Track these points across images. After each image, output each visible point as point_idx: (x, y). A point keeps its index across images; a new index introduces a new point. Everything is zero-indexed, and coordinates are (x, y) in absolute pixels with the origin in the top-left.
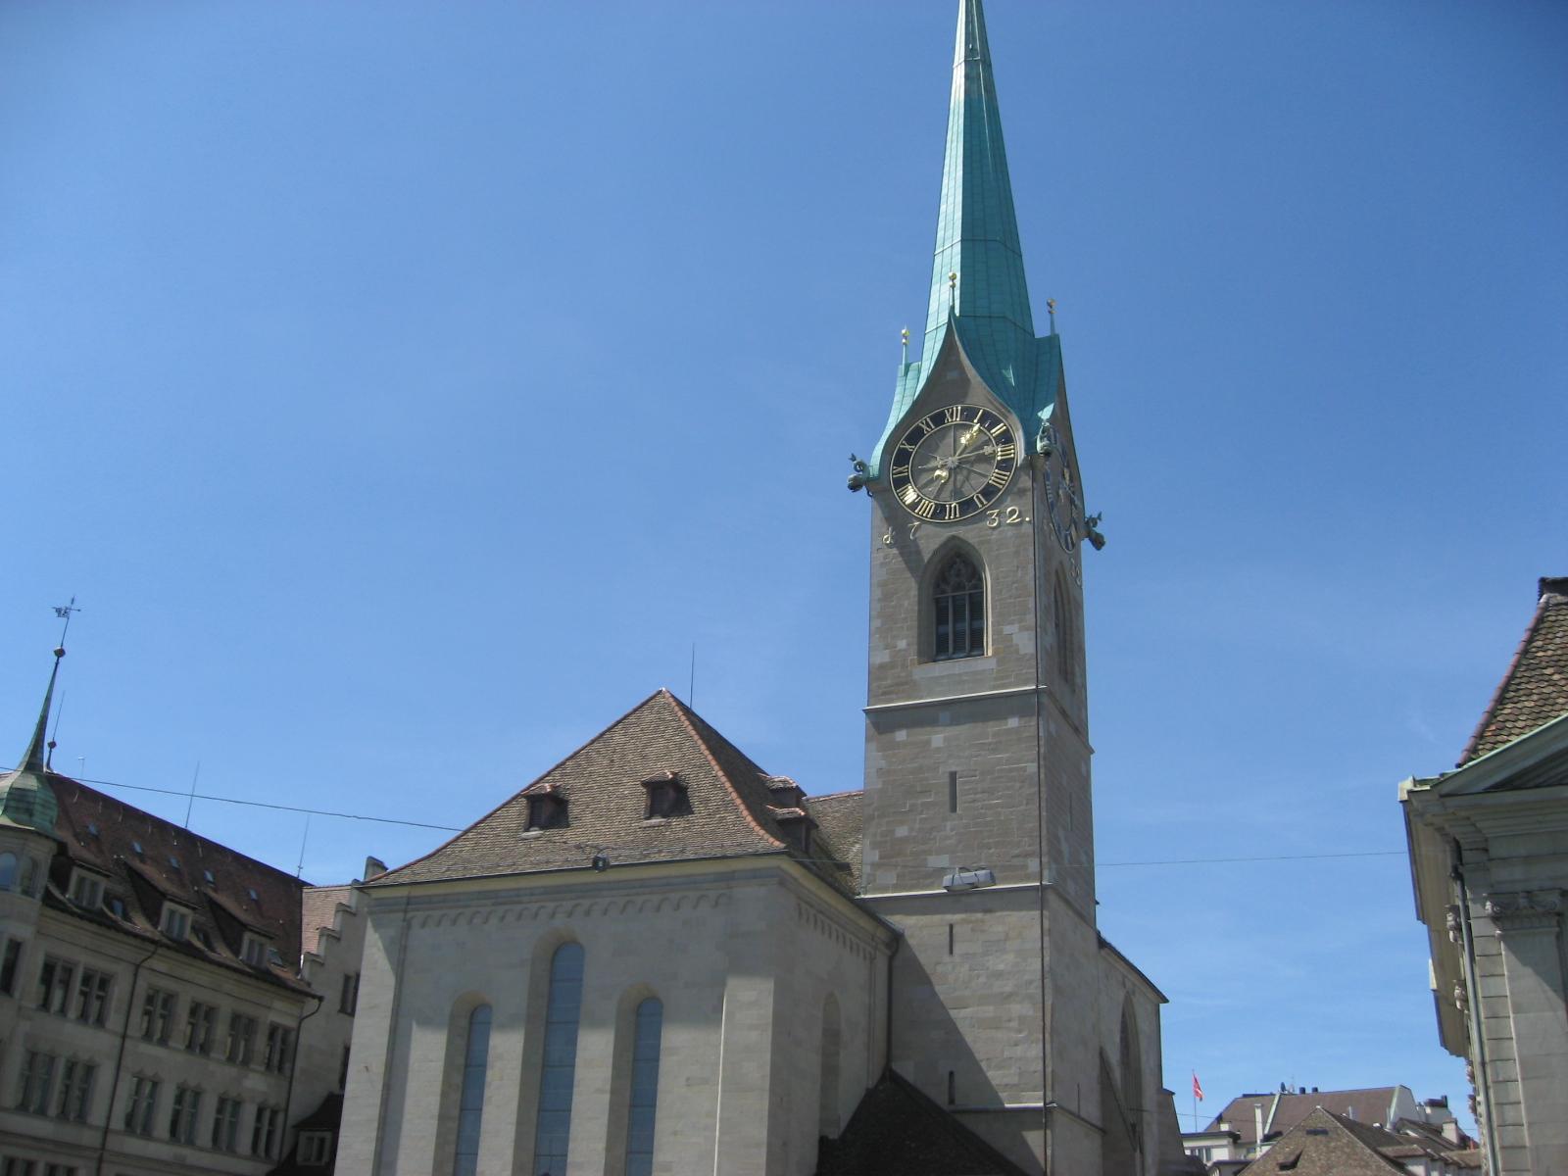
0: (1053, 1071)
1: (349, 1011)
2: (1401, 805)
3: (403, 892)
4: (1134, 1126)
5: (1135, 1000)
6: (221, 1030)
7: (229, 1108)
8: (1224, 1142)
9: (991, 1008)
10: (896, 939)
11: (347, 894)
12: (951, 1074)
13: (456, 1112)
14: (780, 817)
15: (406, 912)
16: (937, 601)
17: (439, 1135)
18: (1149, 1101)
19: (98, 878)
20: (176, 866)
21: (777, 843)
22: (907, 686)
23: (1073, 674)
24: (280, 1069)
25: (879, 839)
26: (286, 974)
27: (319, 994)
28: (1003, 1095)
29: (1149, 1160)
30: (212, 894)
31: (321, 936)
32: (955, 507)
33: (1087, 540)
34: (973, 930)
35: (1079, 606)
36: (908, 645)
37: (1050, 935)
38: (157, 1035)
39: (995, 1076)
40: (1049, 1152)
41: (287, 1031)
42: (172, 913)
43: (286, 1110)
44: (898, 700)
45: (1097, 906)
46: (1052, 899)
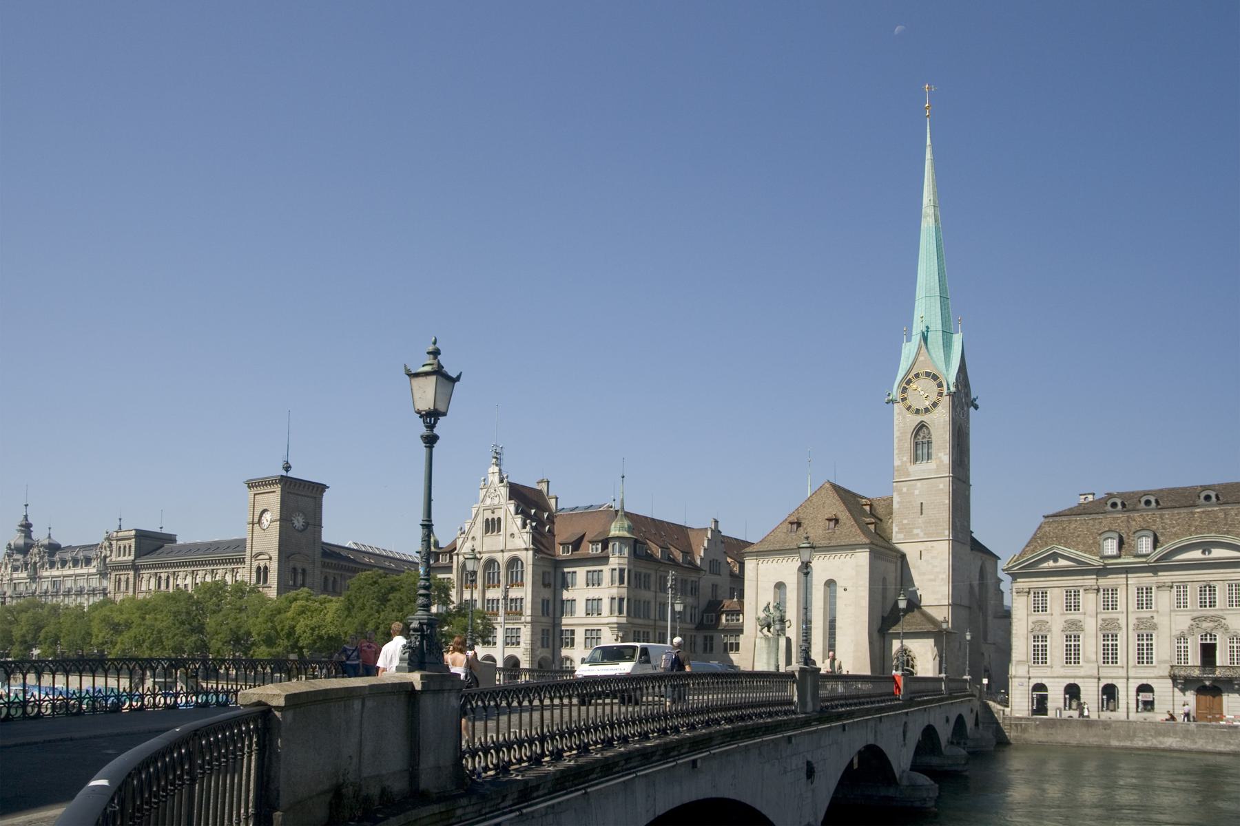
10: (903, 556)
43: (698, 607)
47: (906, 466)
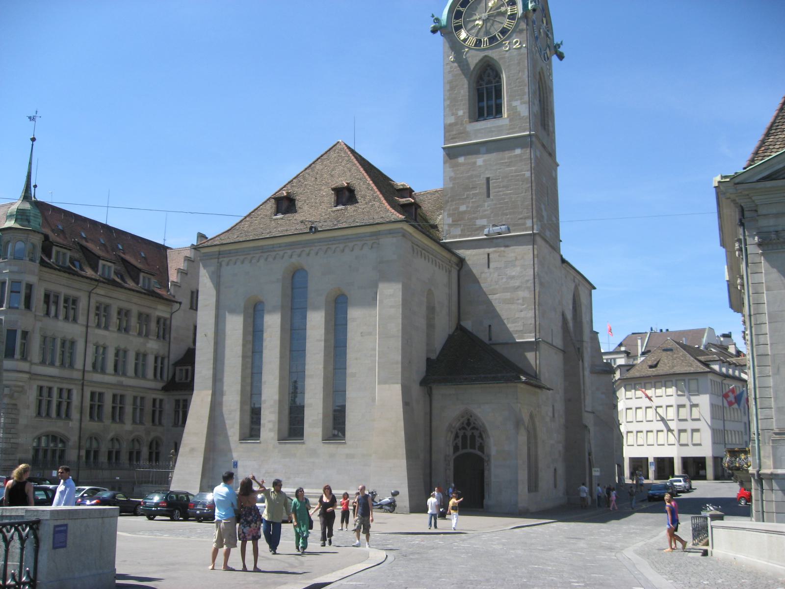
0: (539, 323)
1: (195, 308)
2: (714, 189)
3: (216, 249)
4: (579, 349)
5: (580, 288)
6: (134, 321)
7: (141, 358)
8: (623, 355)
9: (509, 294)
10: (461, 262)
11: (189, 251)
12: (490, 326)
13: (250, 354)
14: (401, 203)
15: (218, 258)
16: (478, 90)
17: (243, 365)
18: (586, 337)
19: (65, 251)
20: (103, 243)
21: (400, 216)
22: (464, 134)
23: (548, 125)
24: (164, 338)
25: (451, 212)
26: (162, 292)
27: (179, 301)
28: (515, 336)
29: (586, 365)
30: (123, 255)
31: (178, 273)
32: (486, 40)
33: (555, 55)
34: (499, 256)
35: (551, 91)
36: (464, 113)
37: (537, 257)
38: (103, 325)
39: (511, 327)
40: (538, 362)
41: (165, 319)
42: (104, 266)
43: (169, 357)
44: (459, 141)
45: (561, 243)
46: (538, 239)
47: (462, 124)
